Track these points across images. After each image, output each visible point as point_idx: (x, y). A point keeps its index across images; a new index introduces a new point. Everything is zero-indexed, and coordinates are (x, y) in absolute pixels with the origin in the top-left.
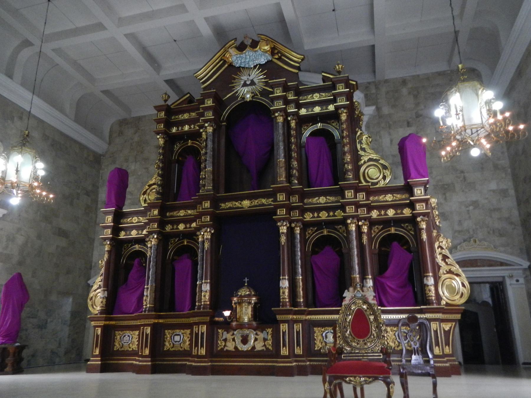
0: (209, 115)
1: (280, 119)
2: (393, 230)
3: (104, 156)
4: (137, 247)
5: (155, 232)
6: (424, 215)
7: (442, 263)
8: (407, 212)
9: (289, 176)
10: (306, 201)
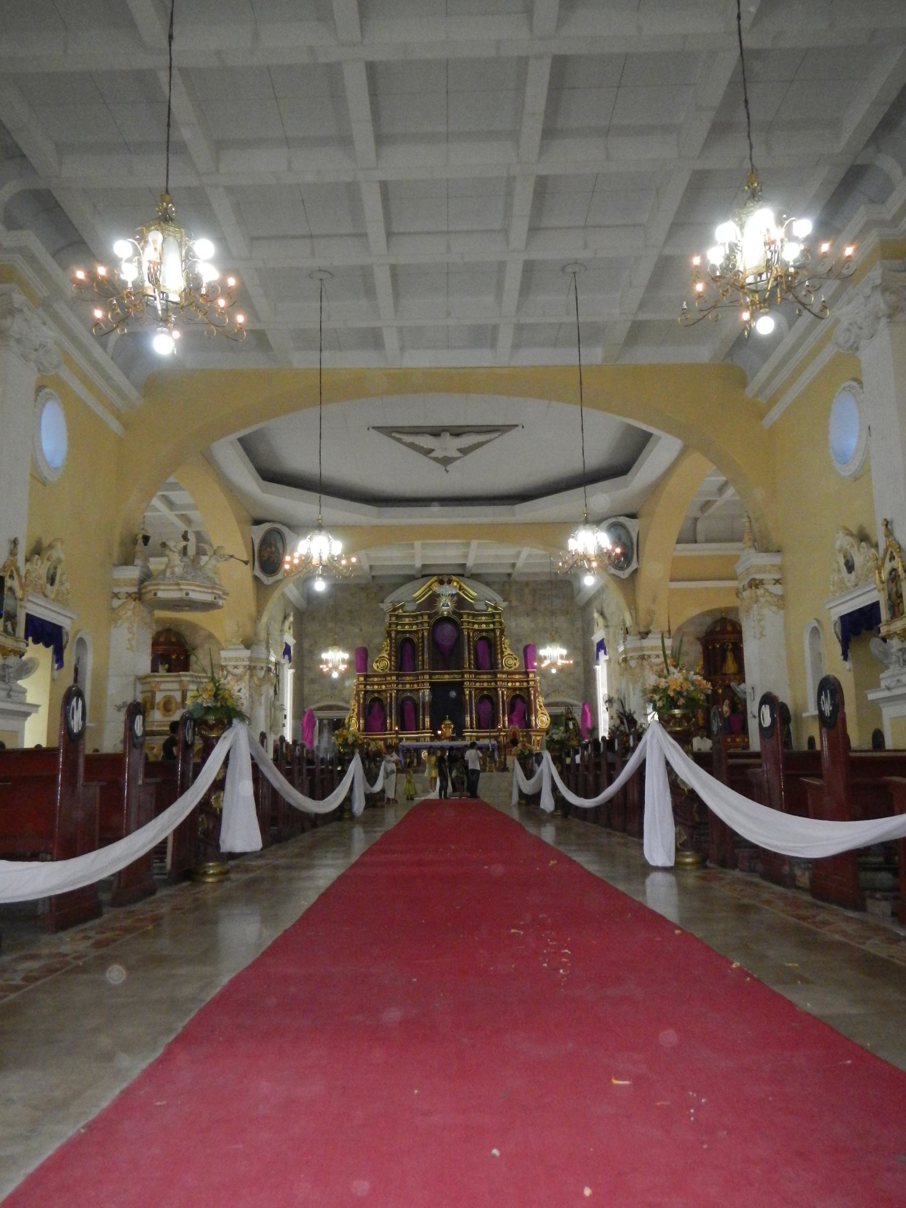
0: (426, 625)
1: (466, 633)
2: (518, 692)
3: (304, 613)
4: (376, 695)
5: (395, 689)
6: (533, 687)
7: (539, 709)
8: (525, 684)
9: (470, 664)
10: (477, 677)
